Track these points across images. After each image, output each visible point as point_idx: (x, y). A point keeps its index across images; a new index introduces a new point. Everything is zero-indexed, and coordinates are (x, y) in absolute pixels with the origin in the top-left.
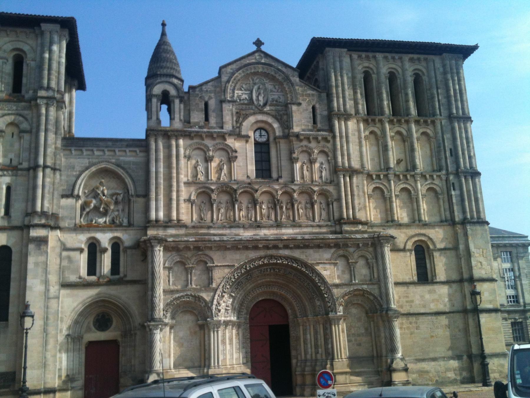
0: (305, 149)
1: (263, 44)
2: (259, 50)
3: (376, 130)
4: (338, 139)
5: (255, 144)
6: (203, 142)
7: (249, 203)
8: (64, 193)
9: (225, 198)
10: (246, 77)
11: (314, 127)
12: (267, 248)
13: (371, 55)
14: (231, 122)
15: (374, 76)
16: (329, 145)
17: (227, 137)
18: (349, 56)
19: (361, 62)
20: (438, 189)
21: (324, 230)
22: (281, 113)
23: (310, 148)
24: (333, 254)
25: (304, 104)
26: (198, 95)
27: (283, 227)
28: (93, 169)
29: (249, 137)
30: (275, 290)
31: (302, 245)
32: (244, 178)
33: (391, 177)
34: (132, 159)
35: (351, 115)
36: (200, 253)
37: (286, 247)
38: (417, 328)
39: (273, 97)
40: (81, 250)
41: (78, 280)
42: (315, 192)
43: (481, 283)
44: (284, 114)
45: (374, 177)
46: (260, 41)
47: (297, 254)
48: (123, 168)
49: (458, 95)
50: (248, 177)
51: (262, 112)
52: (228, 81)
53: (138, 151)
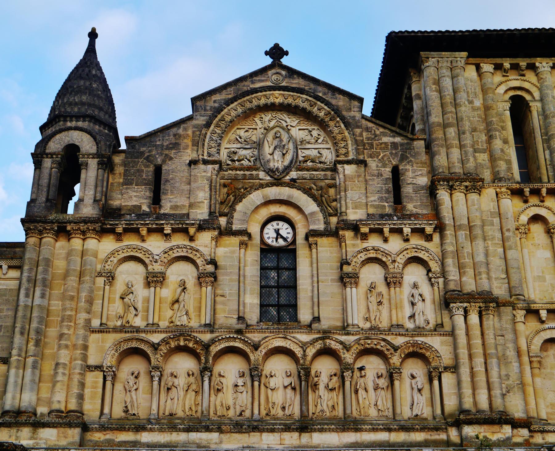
0: (372, 255)
1: (287, 53)
3: (543, 212)
4: (449, 232)
5: (262, 250)
6: (143, 244)
7: (242, 375)
9: (183, 365)
10: (249, 114)
11: (395, 210)
13: (523, 63)
14: (207, 202)
15: (535, 107)
16: (434, 246)
17: (192, 231)
18: (474, 67)
19: (504, 79)
21: (419, 437)
22: (322, 184)
23: (387, 254)
25: (373, 164)
26: (143, 153)
27: (315, 431)
29: (250, 236)
32: (233, 322)
35: (482, 180)
39: (307, 152)
42: (396, 349)
44: (330, 186)
45: (543, 314)
46: (281, 49)
50: (241, 319)
51: (278, 182)
52: (208, 125)
53: (5, 267)
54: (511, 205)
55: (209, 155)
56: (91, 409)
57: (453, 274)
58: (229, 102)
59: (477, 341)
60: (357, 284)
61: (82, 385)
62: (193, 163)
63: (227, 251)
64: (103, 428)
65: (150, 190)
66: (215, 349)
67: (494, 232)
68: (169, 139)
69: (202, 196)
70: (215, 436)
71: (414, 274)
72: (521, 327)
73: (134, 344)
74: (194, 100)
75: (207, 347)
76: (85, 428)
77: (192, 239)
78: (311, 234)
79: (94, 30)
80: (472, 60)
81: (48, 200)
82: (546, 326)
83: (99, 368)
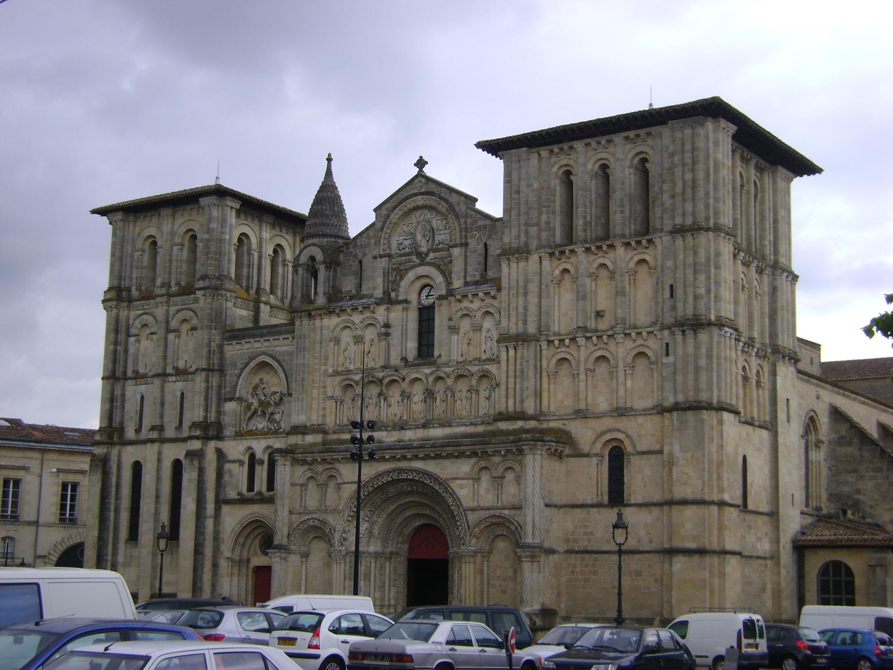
1: (427, 163)
2: (421, 175)
4: (504, 292)
8: (227, 396)
12: (393, 458)
14: (381, 285)
16: (495, 303)
20: (650, 353)
24: (473, 468)
25: (472, 243)
28: (252, 364)
30: (427, 512)
31: (432, 455)
33: (581, 341)
34: (286, 348)
36: (330, 466)
37: (416, 457)
38: (595, 573)
40: (241, 463)
41: (237, 497)
43: (682, 507)
47: (431, 466)
48: (278, 361)
49: (689, 190)
51: (423, 263)
52: (382, 229)
54: (546, 263)
55: (384, 250)
56: (330, 422)
57: (504, 323)
58: (395, 208)
59: (512, 368)
60: (458, 333)
61: (324, 409)
62: (375, 258)
63: (396, 315)
64: (335, 432)
65: (357, 278)
66: (386, 381)
67: (533, 288)
68: (364, 240)
69: (380, 281)
70: (385, 433)
71: (488, 324)
72: (544, 353)
73: (348, 382)
74: (375, 210)
75: (381, 381)
76: (325, 432)
77: (373, 312)
78: (441, 298)
79: (330, 155)
80: (533, 150)
81: (302, 296)
82: (559, 350)
83: (332, 397)
